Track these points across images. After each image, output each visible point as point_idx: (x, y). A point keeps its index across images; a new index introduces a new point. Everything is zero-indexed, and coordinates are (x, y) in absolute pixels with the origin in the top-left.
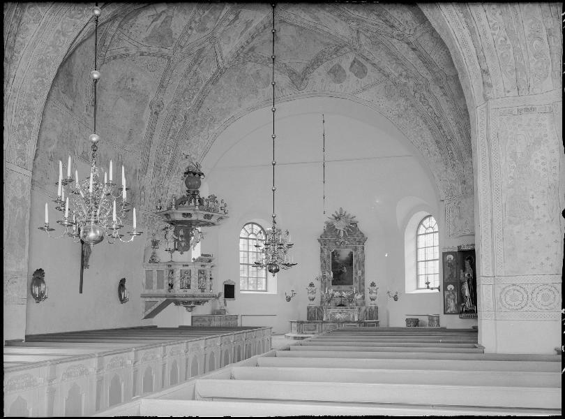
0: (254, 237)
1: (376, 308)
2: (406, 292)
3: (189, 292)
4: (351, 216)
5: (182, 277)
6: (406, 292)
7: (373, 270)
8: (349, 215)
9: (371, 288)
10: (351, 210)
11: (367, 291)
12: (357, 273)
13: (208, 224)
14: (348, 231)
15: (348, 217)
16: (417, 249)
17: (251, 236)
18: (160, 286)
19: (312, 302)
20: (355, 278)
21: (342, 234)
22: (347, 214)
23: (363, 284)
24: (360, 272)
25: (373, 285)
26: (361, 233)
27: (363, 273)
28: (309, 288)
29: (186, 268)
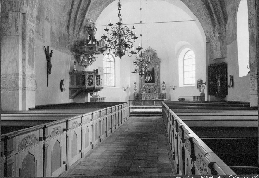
1: (165, 94)
2: (179, 86)
3: (92, 86)
4: (153, 51)
5: (89, 79)
6: (179, 86)
7: (163, 77)
8: (153, 50)
9: (163, 84)
10: (154, 47)
11: (161, 86)
12: (156, 78)
14: (152, 57)
15: (152, 51)
16: (184, 66)
17: (108, 60)
19: (136, 91)
20: (156, 80)
21: (149, 58)
22: (152, 50)
23: (159, 83)
24: (157, 77)
25: (164, 83)
26: (158, 59)
27: (159, 77)
28: (134, 85)
29: (91, 74)
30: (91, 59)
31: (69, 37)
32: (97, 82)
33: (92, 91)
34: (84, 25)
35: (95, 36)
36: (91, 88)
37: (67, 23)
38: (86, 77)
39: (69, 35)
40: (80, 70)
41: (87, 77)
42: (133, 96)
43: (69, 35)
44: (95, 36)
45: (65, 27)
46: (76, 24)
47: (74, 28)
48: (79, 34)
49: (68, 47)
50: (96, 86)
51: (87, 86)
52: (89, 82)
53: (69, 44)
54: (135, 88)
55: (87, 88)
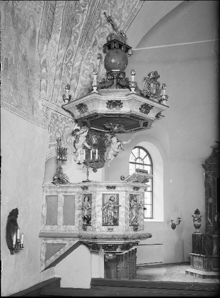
0: (141, 162)
17: (138, 161)
18: (68, 221)
19: (198, 230)
28: (195, 216)
42: (191, 241)
54: (197, 223)
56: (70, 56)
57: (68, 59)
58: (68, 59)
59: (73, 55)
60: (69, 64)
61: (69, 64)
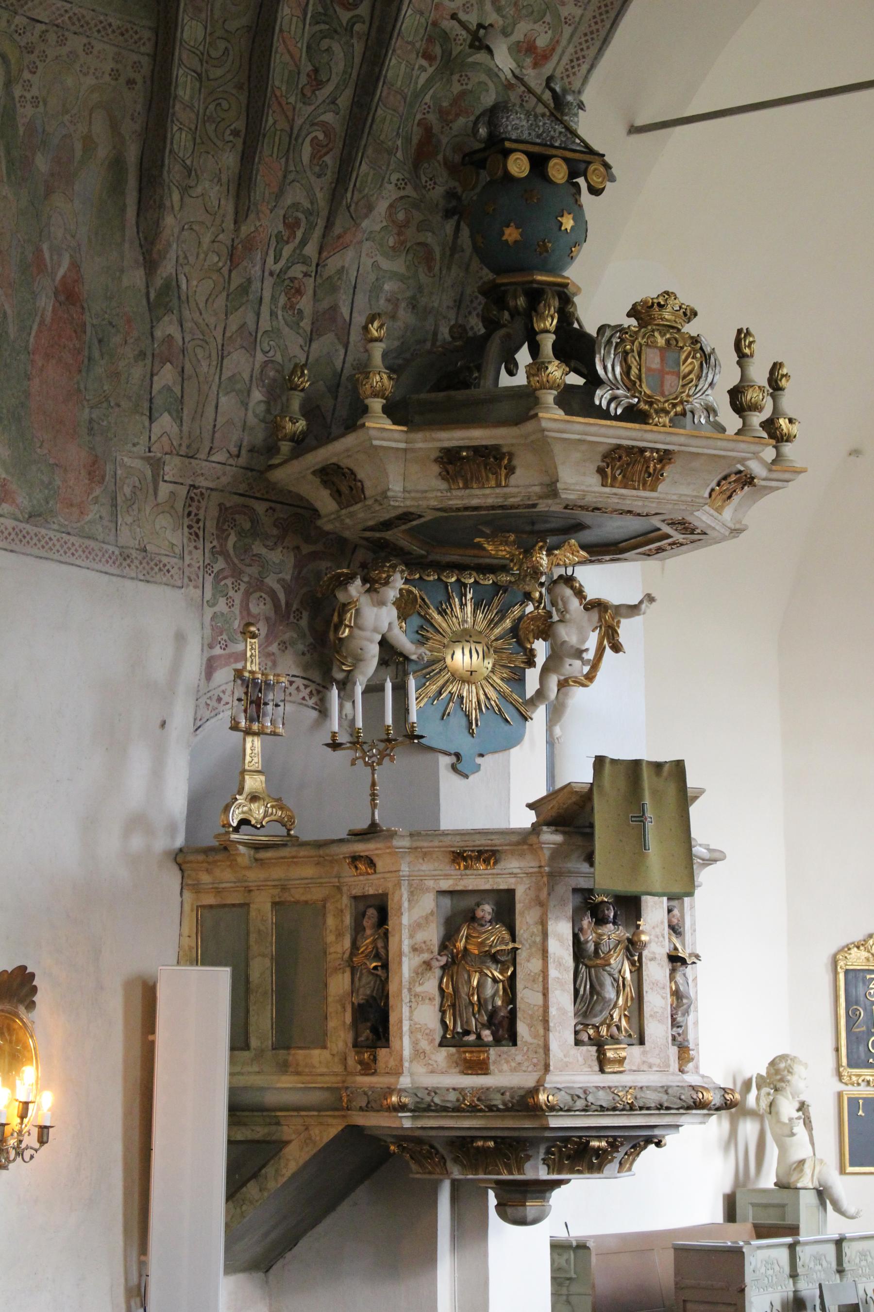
3: (506, 1074)
5: (453, 961)
13: (645, 542)
29: (480, 879)
30: (546, 631)
31: (168, 327)
32: (588, 1000)
33: (512, 1149)
34: (390, 122)
35: (573, 273)
36: (478, 1104)
37: (130, 128)
38: (405, 920)
39: (170, 287)
40: (335, 796)
41: (417, 926)
43: (163, 300)
44: (573, 273)
45: (91, 180)
46: (272, 119)
47: (243, 185)
48: (333, 264)
49: (156, 465)
50: (570, 1071)
51: (420, 1063)
52: (450, 1002)
53: (165, 422)
55: (422, 1109)
56: (299, 234)
57: (287, 251)
58: (287, 251)
59: (311, 227)
60: (297, 271)
61: (297, 271)
